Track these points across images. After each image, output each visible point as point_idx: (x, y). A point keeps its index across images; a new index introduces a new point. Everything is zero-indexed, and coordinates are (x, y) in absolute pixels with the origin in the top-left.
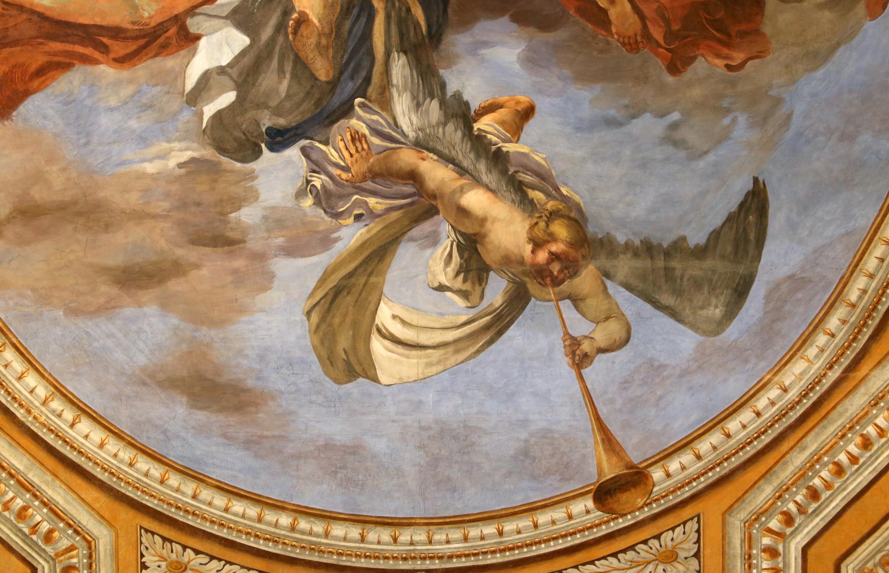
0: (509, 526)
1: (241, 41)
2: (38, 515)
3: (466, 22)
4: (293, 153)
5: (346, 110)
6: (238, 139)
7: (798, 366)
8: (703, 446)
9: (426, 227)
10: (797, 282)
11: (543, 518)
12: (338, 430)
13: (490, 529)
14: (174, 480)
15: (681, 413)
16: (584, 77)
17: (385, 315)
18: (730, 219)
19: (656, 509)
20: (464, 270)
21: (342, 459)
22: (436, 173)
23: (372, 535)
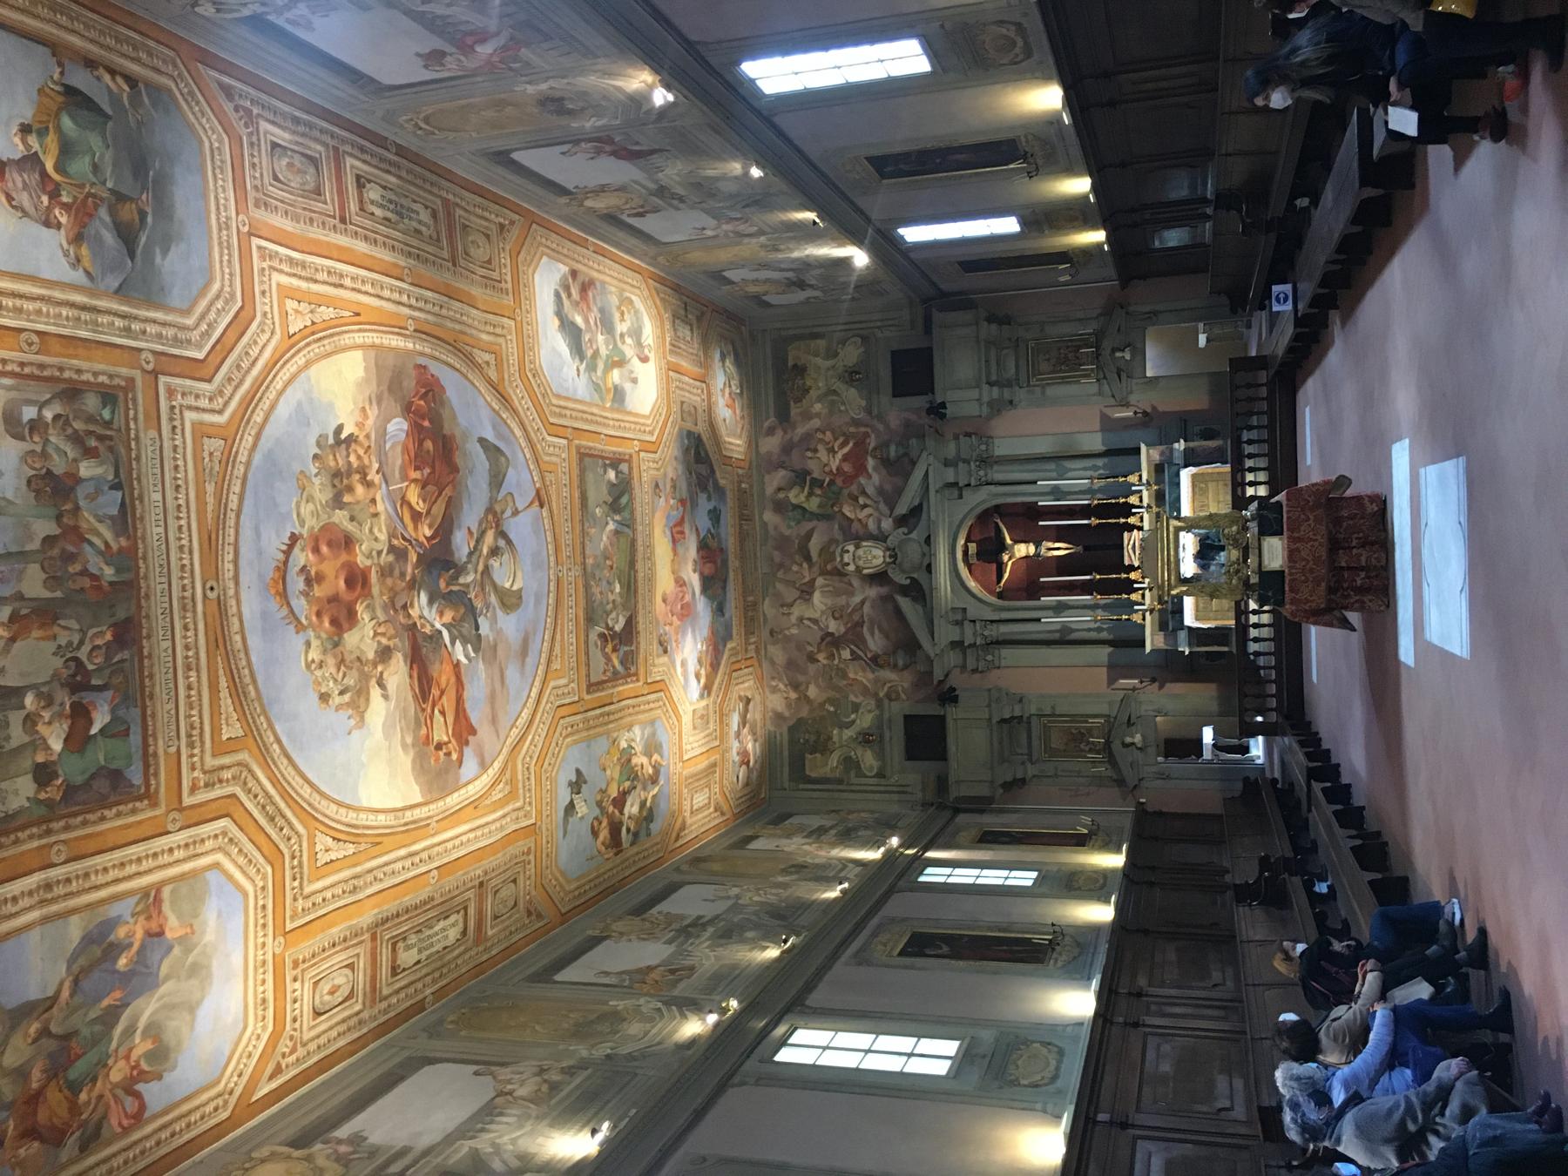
3: (452, 553)
6: (476, 641)
10: (494, 428)
15: (525, 476)
17: (507, 585)
22: (481, 567)
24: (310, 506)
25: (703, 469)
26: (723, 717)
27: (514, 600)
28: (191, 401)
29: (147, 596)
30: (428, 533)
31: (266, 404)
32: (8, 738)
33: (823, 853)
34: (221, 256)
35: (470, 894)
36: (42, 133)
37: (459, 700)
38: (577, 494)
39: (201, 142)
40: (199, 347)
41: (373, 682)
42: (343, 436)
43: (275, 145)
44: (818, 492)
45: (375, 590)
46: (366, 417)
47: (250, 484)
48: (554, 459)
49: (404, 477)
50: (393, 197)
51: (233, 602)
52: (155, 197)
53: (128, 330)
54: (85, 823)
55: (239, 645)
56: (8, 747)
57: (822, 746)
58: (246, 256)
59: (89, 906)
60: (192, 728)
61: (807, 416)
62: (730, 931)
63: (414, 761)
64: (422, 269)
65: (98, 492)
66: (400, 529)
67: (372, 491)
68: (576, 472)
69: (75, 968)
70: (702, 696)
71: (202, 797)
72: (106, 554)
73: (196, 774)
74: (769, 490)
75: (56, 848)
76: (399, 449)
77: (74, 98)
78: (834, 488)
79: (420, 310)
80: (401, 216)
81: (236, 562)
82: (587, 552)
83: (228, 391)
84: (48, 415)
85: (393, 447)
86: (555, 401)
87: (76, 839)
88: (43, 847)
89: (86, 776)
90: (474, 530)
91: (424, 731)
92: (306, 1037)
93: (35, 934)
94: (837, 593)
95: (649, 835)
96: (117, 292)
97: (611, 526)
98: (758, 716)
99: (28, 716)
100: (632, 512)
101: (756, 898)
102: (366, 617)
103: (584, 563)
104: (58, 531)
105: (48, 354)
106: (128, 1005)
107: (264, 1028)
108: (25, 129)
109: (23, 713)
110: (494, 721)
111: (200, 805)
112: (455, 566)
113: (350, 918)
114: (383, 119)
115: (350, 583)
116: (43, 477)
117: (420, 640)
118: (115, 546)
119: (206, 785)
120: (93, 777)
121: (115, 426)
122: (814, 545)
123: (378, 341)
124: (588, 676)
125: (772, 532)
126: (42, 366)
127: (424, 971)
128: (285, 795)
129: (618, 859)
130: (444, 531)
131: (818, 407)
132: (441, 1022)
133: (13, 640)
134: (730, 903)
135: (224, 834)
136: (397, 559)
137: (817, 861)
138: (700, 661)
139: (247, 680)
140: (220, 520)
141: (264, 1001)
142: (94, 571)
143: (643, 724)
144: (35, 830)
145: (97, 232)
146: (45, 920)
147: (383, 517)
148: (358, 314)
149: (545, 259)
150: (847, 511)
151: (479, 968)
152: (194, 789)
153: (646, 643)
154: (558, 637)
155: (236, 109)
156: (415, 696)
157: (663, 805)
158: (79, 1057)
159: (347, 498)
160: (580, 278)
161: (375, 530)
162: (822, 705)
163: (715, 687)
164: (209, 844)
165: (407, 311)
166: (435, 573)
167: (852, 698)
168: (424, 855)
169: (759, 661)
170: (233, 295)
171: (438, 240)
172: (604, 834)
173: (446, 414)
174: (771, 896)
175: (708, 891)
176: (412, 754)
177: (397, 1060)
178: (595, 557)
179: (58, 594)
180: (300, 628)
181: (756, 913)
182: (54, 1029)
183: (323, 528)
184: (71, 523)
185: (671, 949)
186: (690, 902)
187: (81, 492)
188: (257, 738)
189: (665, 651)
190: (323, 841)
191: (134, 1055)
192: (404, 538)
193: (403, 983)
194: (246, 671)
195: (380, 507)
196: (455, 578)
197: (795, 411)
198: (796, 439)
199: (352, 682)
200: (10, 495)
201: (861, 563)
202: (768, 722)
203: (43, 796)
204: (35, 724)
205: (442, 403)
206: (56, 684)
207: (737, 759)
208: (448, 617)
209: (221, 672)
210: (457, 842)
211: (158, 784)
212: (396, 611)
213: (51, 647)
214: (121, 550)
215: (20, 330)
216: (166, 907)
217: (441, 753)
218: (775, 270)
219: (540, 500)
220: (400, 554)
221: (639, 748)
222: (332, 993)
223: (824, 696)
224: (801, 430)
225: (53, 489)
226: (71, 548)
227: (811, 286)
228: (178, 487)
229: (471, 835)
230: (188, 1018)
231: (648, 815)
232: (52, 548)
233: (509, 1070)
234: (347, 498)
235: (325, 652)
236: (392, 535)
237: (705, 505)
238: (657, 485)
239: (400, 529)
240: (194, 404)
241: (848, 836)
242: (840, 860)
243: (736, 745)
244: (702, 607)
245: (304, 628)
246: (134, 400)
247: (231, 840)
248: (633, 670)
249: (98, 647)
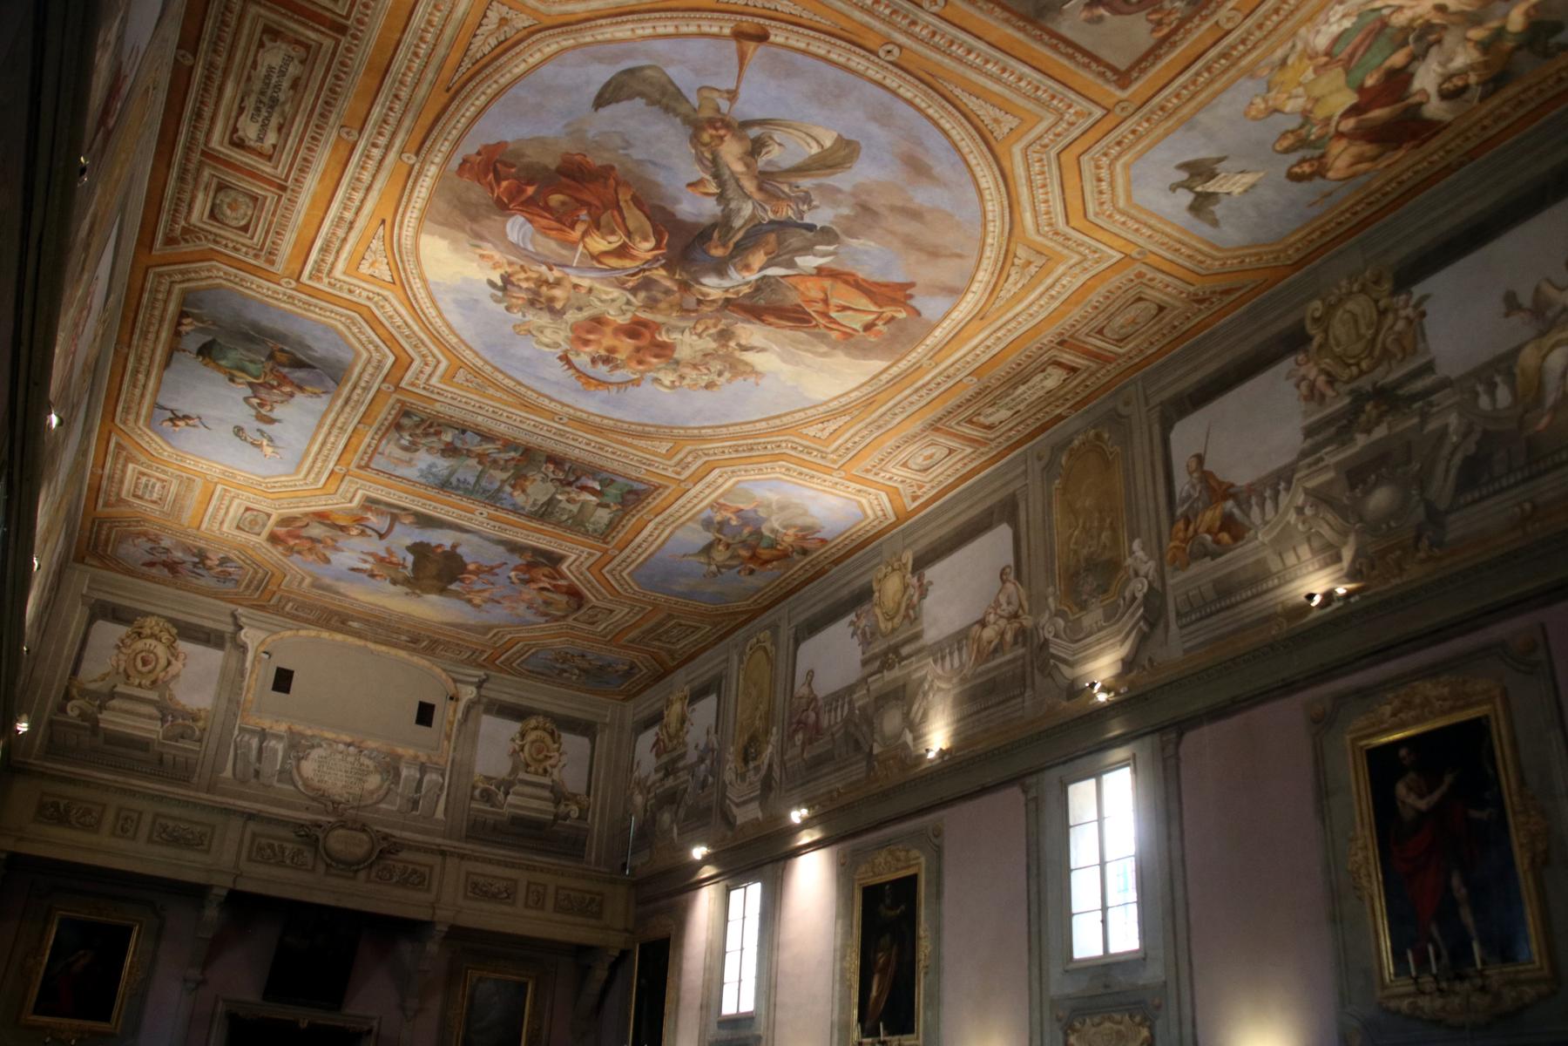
0: (822, 52)
1: (799, 260)
2: (1036, 168)
3: (695, 225)
4: (807, 220)
5: (771, 222)
6: (828, 235)
7: (619, 35)
8: (693, 29)
9: (769, 169)
10: (600, 60)
11: (802, 45)
12: (873, 128)
13: (833, 56)
14: (966, 150)
15: (696, 48)
16: (656, 185)
17: (815, 150)
18: (617, 101)
19: (739, 17)
20: (764, 145)
21: (883, 117)
22: (749, 186)
23: (894, 85)
24: (548, 332)
28: (424, 377)
30: (651, 244)
31: (445, 331)
40: (385, 356)
42: (500, 283)
45: (659, 318)
46: (490, 257)
47: (502, 368)
58: (315, 293)
63: (848, 354)
67: (566, 283)
76: (540, 238)
81: (552, 400)
85: (533, 241)
102: (676, 336)
117: (747, 302)
128: (744, 438)
130: (663, 221)
147: (597, 285)
148: (383, 222)
154: (972, 103)
161: (604, 297)
165: (392, 155)
170: (349, 317)
173: (533, 156)
180: (635, 383)
195: (586, 283)
212: (695, 311)
217: (880, 326)
234: (558, 305)
236: (621, 285)
239: (621, 275)
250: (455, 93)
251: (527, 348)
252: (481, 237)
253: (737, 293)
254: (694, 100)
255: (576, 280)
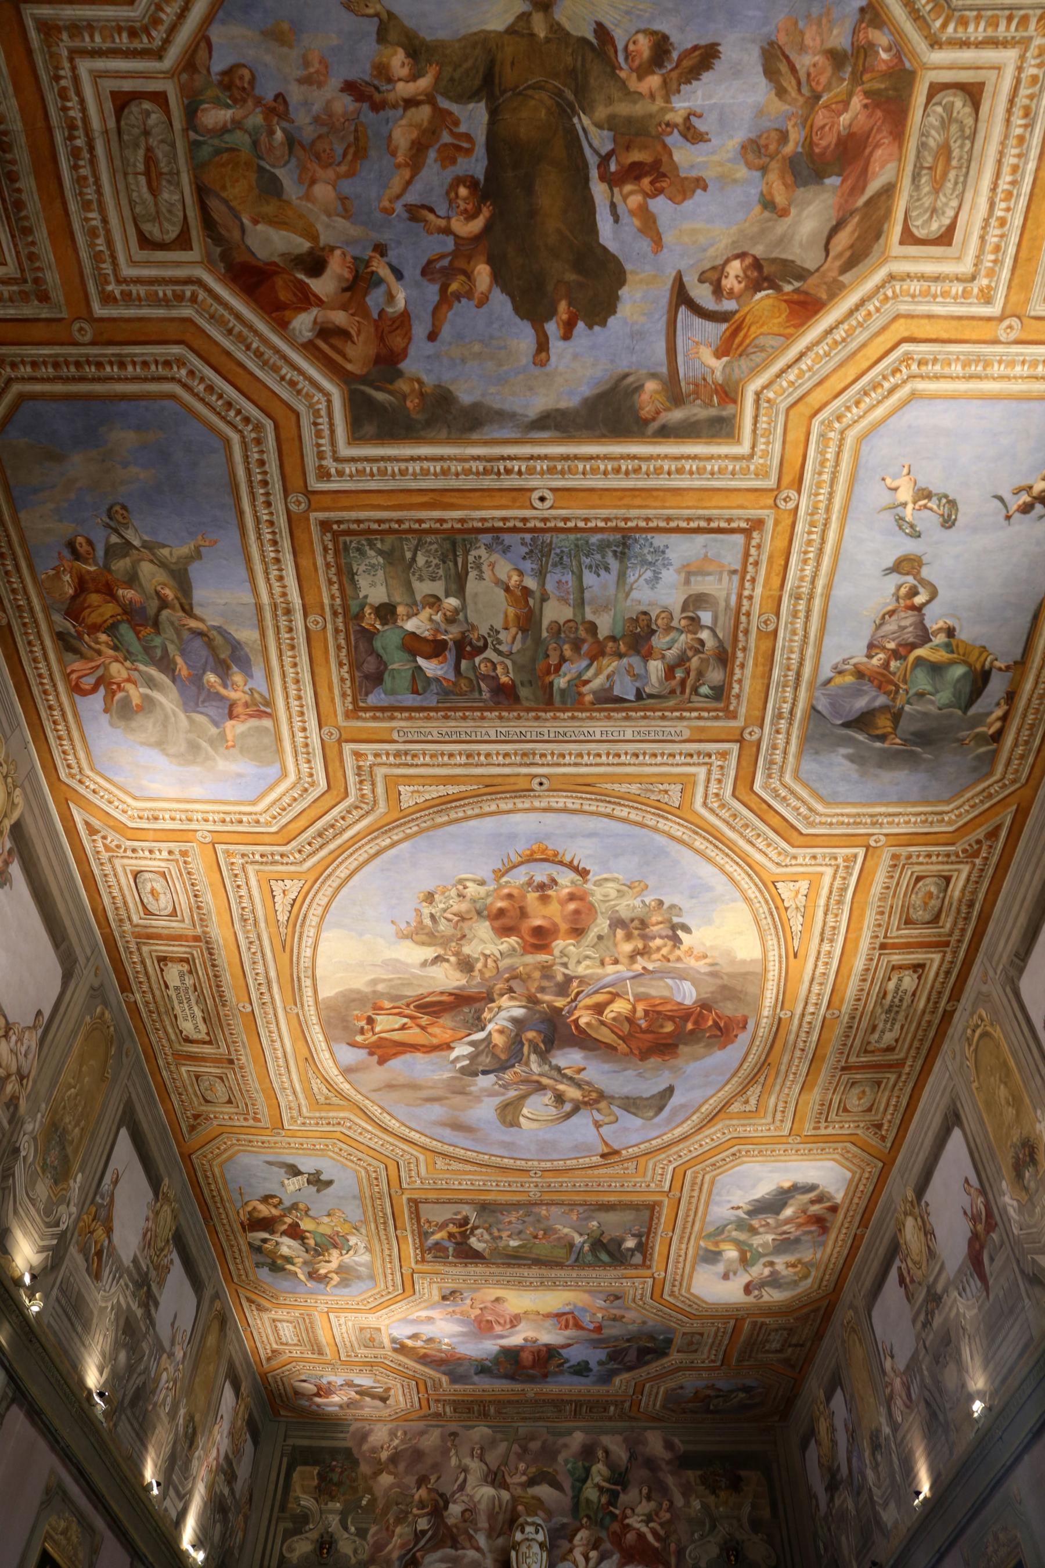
3: (561, 1047)
6: (470, 1072)
10: (683, 1106)
12: (507, 1138)
15: (634, 1139)
17: (525, 1111)
22: (545, 1081)
24: (613, 894)
25: (632, 1356)
26: (370, 1365)
27: (509, 1118)
28: (715, 776)
29: (537, 718)
30: (582, 1021)
31: (712, 852)
32: (421, 579)
33: (203, 1472)
34: (848, 815)
35: (223, 1050)
36: (948, 647)
37: (414, 1047)
38: (613, 1199)
39: (948, 802)
40: (765, 786)
41: (440, 951)
42: (679, 933)
43: (948, 879)
44: (604, 1500)
45: (530, 959)
46: (698, 958)
47: (637, 830)
48: (650, 1173)
49: (638, 998)
50: (905, 1004)
51: (527, 805)
52: (898, 752)
53: (780, 716)
54: (339, 648)
55: (486, 809)
56: (413, 579)
57: (325, 1489)
58: (848, 841)
59: (265, 648)
60: (414, 756)
61: (687, 1491)
62: (131, 1334)
63: (359, 992)
64: (838, 1031)
65: (636, 677)
66: (588, 989)
67: (625, 961)
68: (635, 1198)
69: (214, 633)
70: (394, 1341)
71: (349, 762)
72: (580, 681)
73: (371, 758)
74: (606, 1440)
75: (320, 619)
76: (666, 993)
77: (980, 679)
78: (607, 1520)
79: (800, 1026)
80: (889, 1011)
81: (565, 810)
82: (553, 1209)
83: (724, 814)
84: (704, 635)
86: (707, 1177)
87: (326, 639)
88: (322, 608)
89: (381, 652)
90: (582, 1076)
91: (387, 1004)
92: (117, 862)
93: (249, 599)
94: (492, 1516)
95: (258, 1265)
96: (813, 708)
97: (578, 1240)
98: (366, 1412)
99: (438, 599)
100: (590, 1265)
101: (165, 1376)
102: (504, 947)
103: (541, 1203)
104: (601, 637)
105: (759, 639)
106: (174, 681)
107: (132, 818)
108: (950, 632)
109: (441, 594)
110: (390, 1087)
111: (342, 760)
112: (548, 1051)
113: (219, 914)
114: (980, 993)
115: (539, 932)
116: (649, 626)
117: (477, 1005)
118: (585, 689)
119: (359, 768)
120: (379, 656)
121: (694, 698)
122: (543, 1491)
123: (770, 976)
124: (426, 1201)
125: (561, 1441)
126: (746, 632)
127: (157, 993)
128: (342, 849)
129: (237, 1227)
130: (583, 1040)
131: (696, 1504)
132: (106, 1004)
133: (507, 589)
134: (166, 1344)
135: (312, 784)
136: (558, 985)
137: (195, 1463)
138: (431, 1340)
139: (453, 815)
140: (605, 797)
141: (156, 819)
142: (565, 668)
143: (371, 1266)
144: (338, 601)
145: (866, 693)
146: (259, 607)
147: (600, 971)
148: (795, 956)
149: (849, 1175)
150: (582, 1535)
151: (151, 1056)
152: (357, 755)
153: (456, 1274)
154: (468, 1167)
155: (978, 842)
156: (422, 997)
157: (286, 1284)
158: (137, 633)
159: (620, 933)
160: (828, 1216)
161: (588, 962)
162: (369, 1490)
163: (402, 1358)
164: (304, 767)
166: (542, 1027)
167: (373, 1529)
168: (266, 998)
169: (424, 1418)
170: (812, 824)
171: (866, 1052)
172: (265, 1211)
173: (699, 1049)
174: (164, 1396)
175: (186, 1323)
176: (367, 989)
177: (78, 951)
178: (547, 1218)
179: (545, 634)
180: (499, 874)
181: (147, 1369)
182: (165, 613)
183: (591, 907)
184: (608, 650)
185: (127, 1261)
186: (176, 1299)
187: (635, 660)
188: (399, 822)
189: (444, 1298)
190: (293, 887)
191: (129, 686)
192: (578, 994)
193: (150, 969)
194: (461, 814)
195: (610, 969)
196: (535, 1049)
197: (691, 1475)
198: (661, 1475)
199: (442, 928)
200: (635, 594)
201: (523, 1548)
202: (359, 1424)
203: (367, 610)
204: (431, 606)
205: (709, 1046)
206: (465, 627)
207: (324, 1381)
208: (498, 1040)
209: (463, 788)
210: (275, 1036)
211: (365, 719)
212: (508, 980)
213: (498, 625)
214: (581, 695)
215: (778, 615)
216: (254, 722)
217: (363, 1023)
218: (849, 1452)
219: (609, 1154)
220: (563, 989)
221: (347, 1259)
222: (153, 892)
223: (379, 1492)
224: (670, 1480)
225: (639, 636)
226: (585, 647)
227: (832, 1500)
228: (637, 755)
229: (280, 1053)
230: (153, 740)
231: (277, 1265)
232: (587, 630)
233: (34, 1045)
235: (474, 901)
236: (582, 980)
237: (595, 1356)
238: (617, 1298)
239: (588, 989)
240: (713, 777)
241: (218, 1509)
242: (190, 1493)
243: (338, 1380)
244: (488, 1347)
245: (497, 879)
246: (717, 718)
247: (306, 790)
248: (428, 1257)
249: (495, 669)
250: (764, 1064)
251: (624, 868)
252: (714, 974)
253: (491, 1010)
254: (615, 1109)
255: (619, 967)
